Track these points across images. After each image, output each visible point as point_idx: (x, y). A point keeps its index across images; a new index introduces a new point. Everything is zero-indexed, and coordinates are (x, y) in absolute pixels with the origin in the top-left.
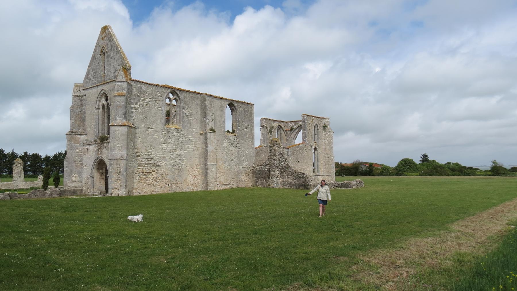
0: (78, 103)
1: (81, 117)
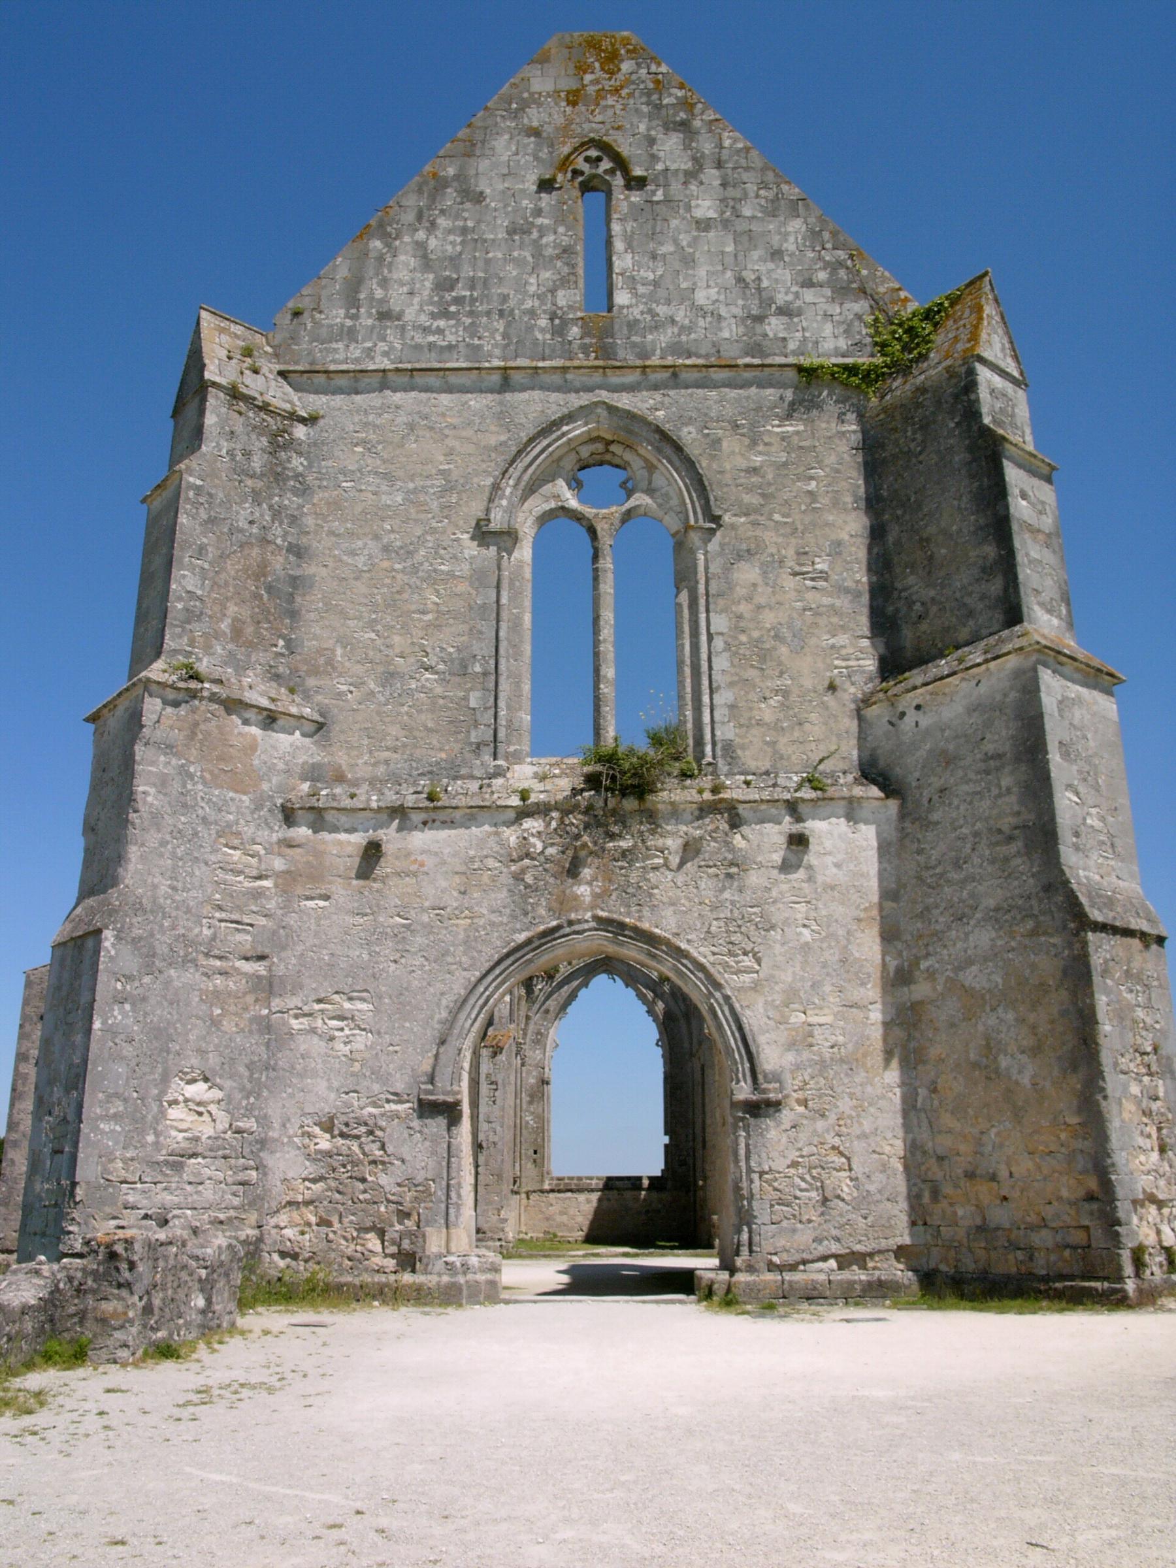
0: (247, 454)
1: (262, 569)
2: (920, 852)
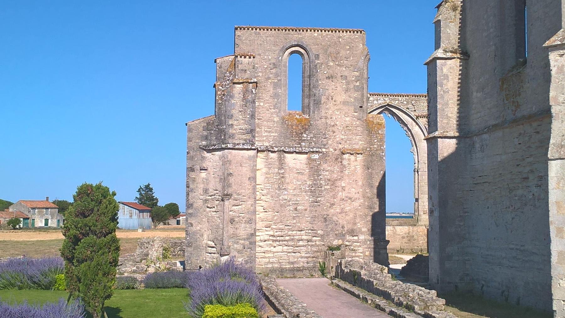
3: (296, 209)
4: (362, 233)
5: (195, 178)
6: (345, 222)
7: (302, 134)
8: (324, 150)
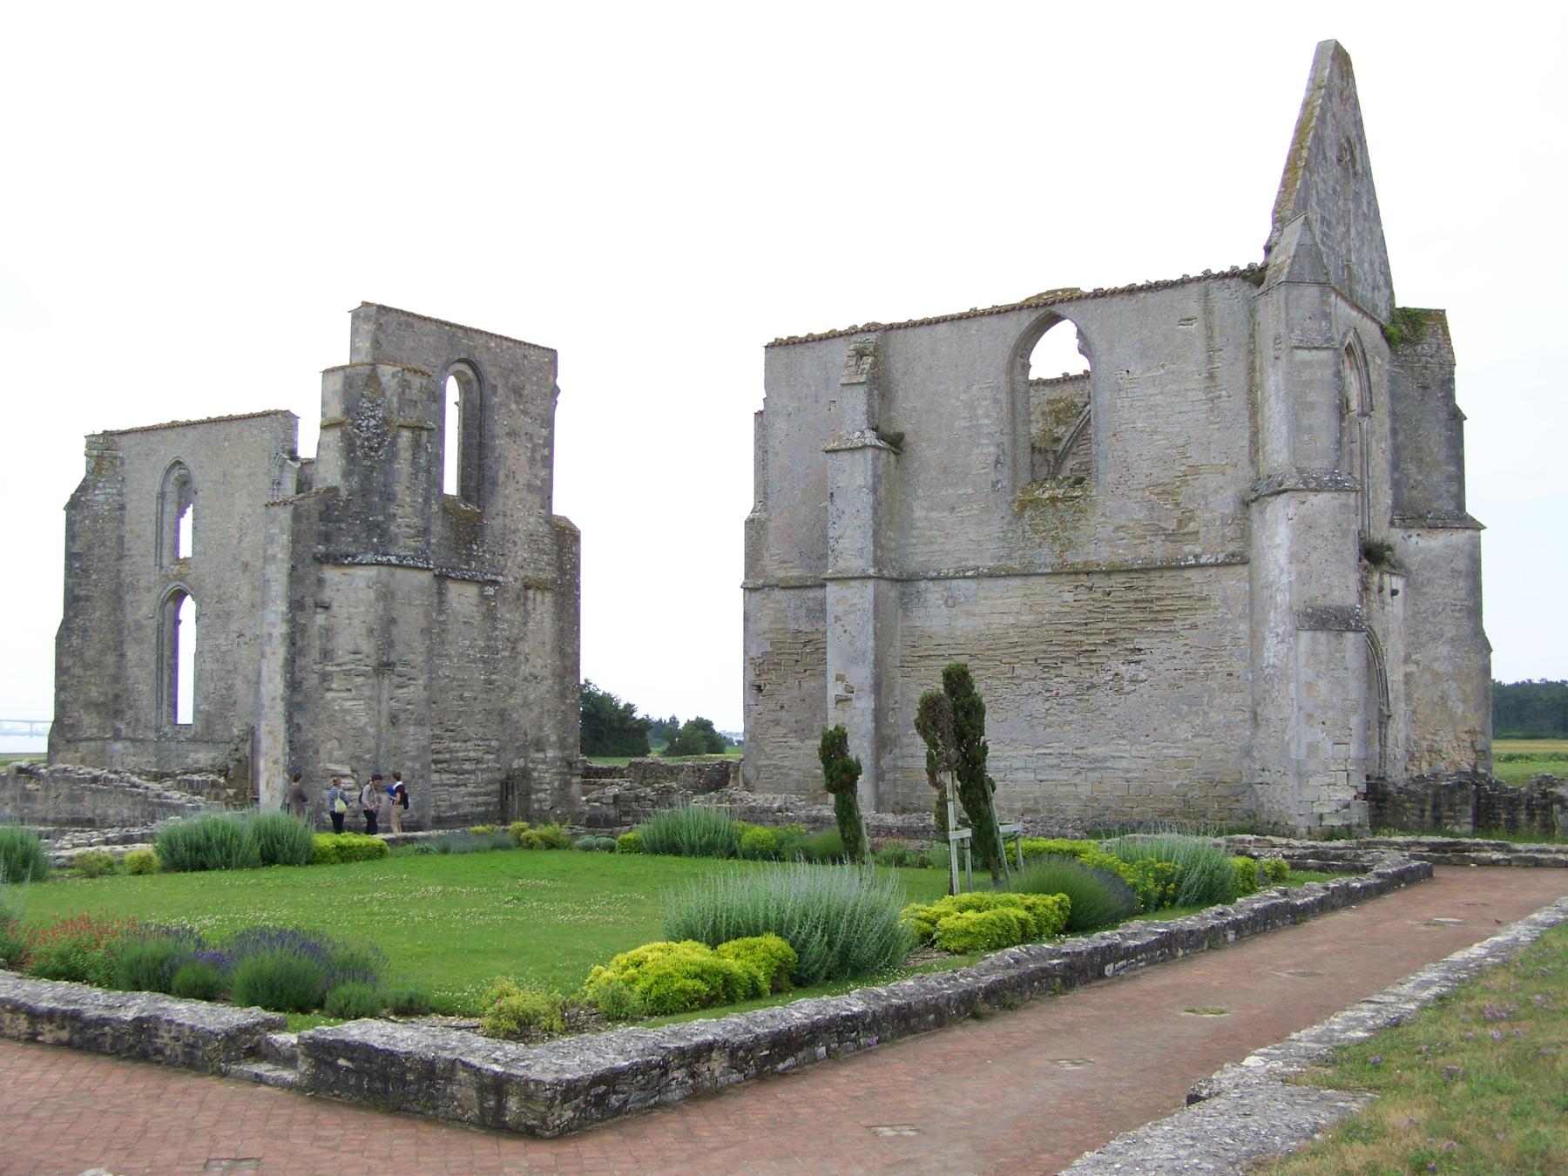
2: (1415, 605)
3: (462, 698)
4: (551, 745)
5: (305, 625)
6: (528, 725)
7: (471, 543)
8: (500, 579)
